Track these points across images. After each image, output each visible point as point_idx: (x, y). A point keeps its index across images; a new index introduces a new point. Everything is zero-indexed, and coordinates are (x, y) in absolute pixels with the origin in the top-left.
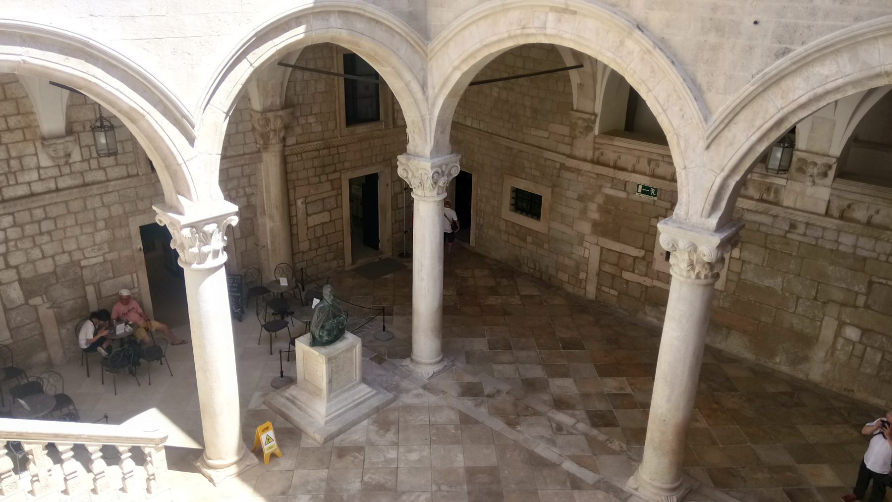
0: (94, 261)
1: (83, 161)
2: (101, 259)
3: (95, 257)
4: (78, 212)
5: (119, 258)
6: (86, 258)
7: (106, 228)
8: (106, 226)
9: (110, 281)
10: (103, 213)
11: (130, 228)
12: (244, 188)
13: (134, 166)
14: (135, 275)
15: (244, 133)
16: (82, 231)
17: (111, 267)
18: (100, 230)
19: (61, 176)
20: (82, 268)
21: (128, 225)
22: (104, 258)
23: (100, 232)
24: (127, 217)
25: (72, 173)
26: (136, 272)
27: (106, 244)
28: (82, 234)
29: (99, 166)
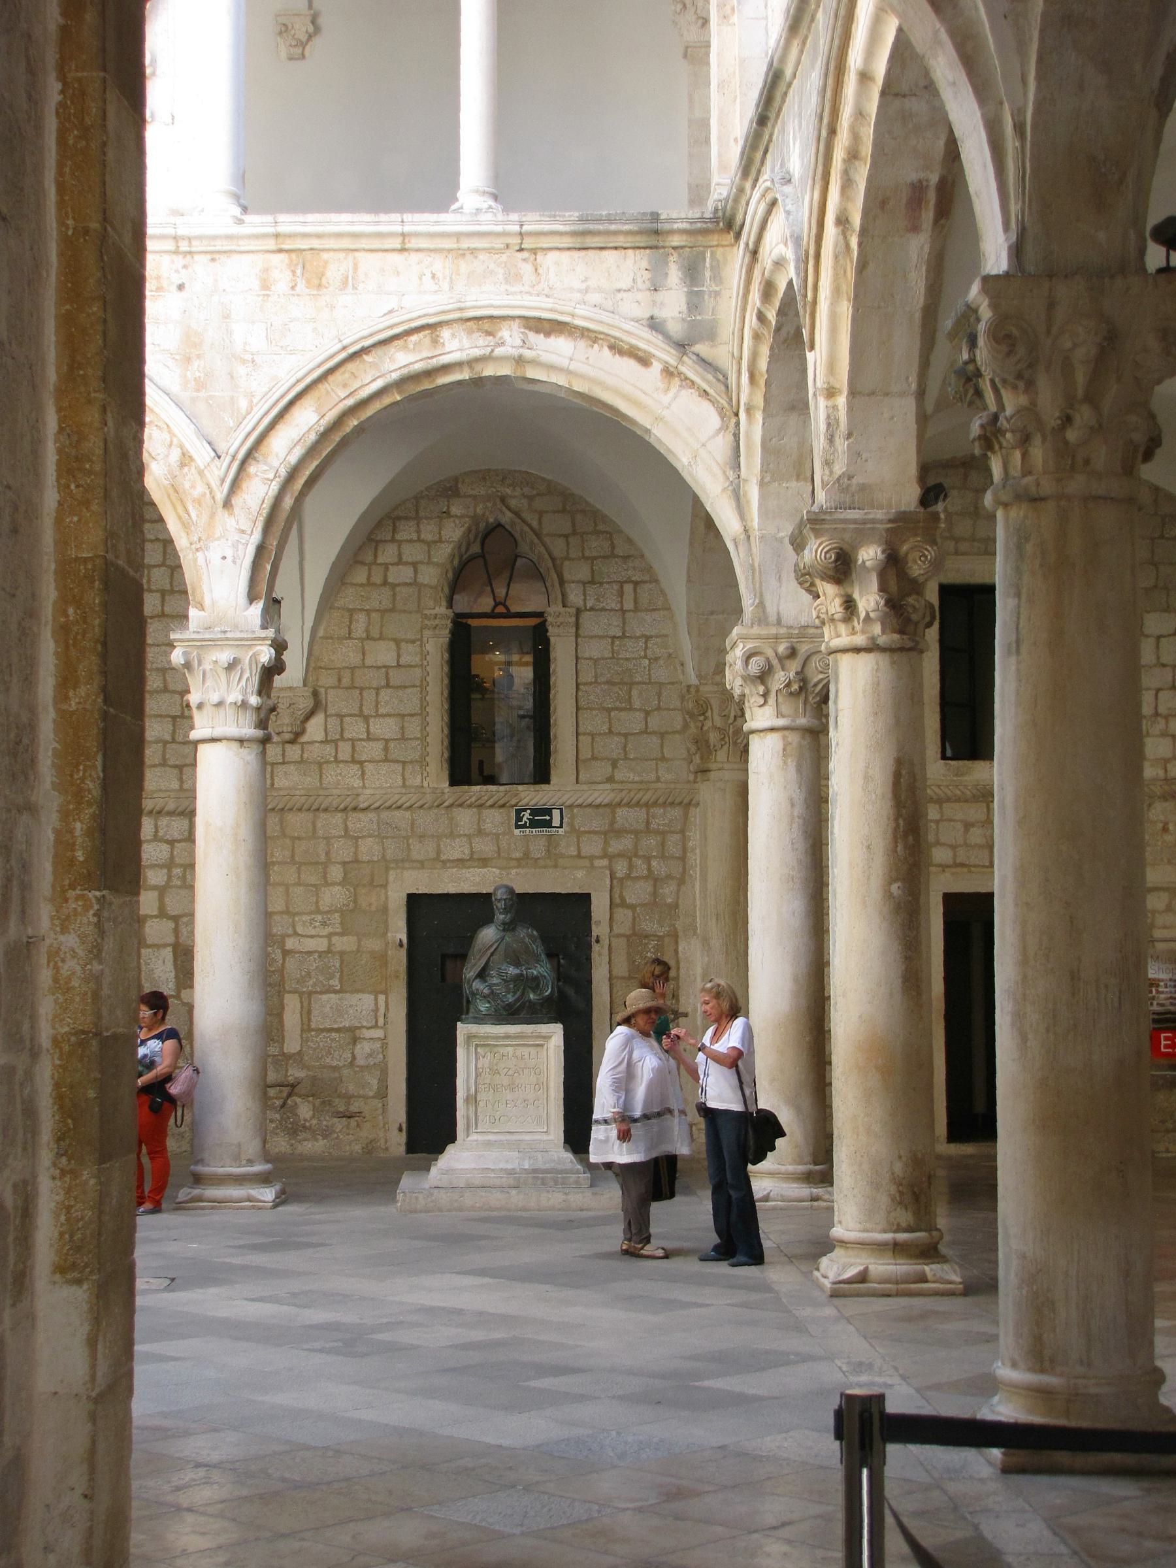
0: (310, 944)
1: (326, 742)
2: (322, 945)
3: (312, 937)
4: (299, 838)
5: (358, 951)
6: (296, 934)
7: (344, 882)
8: (344, 878)
9: (332, 995)
10: (342, 850)
11: (390, 893)
12: (648, 859)
13: (417, 768)
14: (381, 998)
15: (662, 735)
16: (299, 877)
17: (338, 965)
18: (334, 884)
19: (284, 763)
20: (286, 953)
21: (385, 886)
22: (330, 945)
23: (331, 888)
24: (387, 869)
25: (302, 761)
26: (385, 992)
27: (337, 915)
28: (299, 884)
29: (353, 756)
